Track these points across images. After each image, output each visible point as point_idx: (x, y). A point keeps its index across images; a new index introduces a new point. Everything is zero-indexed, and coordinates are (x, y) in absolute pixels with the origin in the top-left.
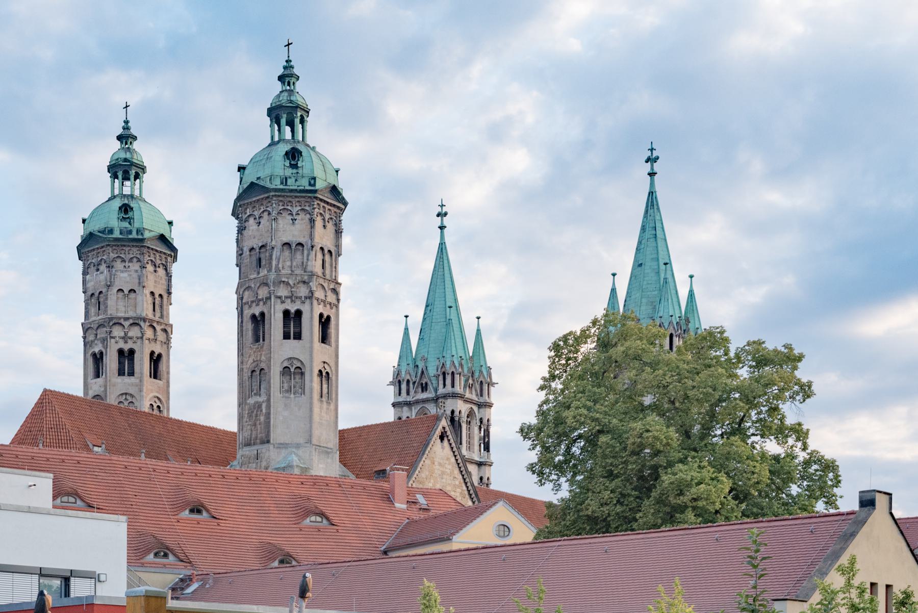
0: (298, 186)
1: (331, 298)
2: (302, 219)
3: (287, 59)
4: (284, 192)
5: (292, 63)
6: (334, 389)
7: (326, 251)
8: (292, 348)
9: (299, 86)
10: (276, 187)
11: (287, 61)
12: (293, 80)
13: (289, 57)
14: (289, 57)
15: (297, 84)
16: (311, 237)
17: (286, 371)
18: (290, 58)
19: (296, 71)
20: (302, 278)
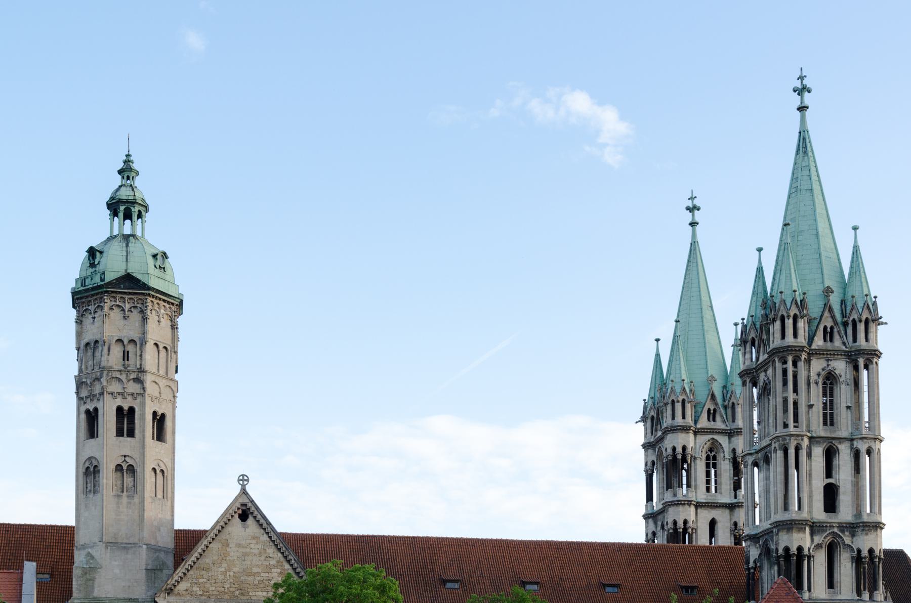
0: (93, 284)
1: (133, 387)
2: (135, 316)
3: (127, 153)
4: (81, 294)
5: (132, 158)
6: (169, 482)
7: (161, 347)
8: (127, 445)
9: (138, 182)
10: (79, 290)
11: (127, 156)
12: (133, 174)
13: (129, 151)
14: (129, 151)
15: (137, 179)
16: (144, 333)
17: (119, 468)
18: (130, 153)
19: (135, 166)
20: (96, 375)
